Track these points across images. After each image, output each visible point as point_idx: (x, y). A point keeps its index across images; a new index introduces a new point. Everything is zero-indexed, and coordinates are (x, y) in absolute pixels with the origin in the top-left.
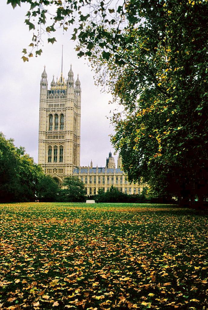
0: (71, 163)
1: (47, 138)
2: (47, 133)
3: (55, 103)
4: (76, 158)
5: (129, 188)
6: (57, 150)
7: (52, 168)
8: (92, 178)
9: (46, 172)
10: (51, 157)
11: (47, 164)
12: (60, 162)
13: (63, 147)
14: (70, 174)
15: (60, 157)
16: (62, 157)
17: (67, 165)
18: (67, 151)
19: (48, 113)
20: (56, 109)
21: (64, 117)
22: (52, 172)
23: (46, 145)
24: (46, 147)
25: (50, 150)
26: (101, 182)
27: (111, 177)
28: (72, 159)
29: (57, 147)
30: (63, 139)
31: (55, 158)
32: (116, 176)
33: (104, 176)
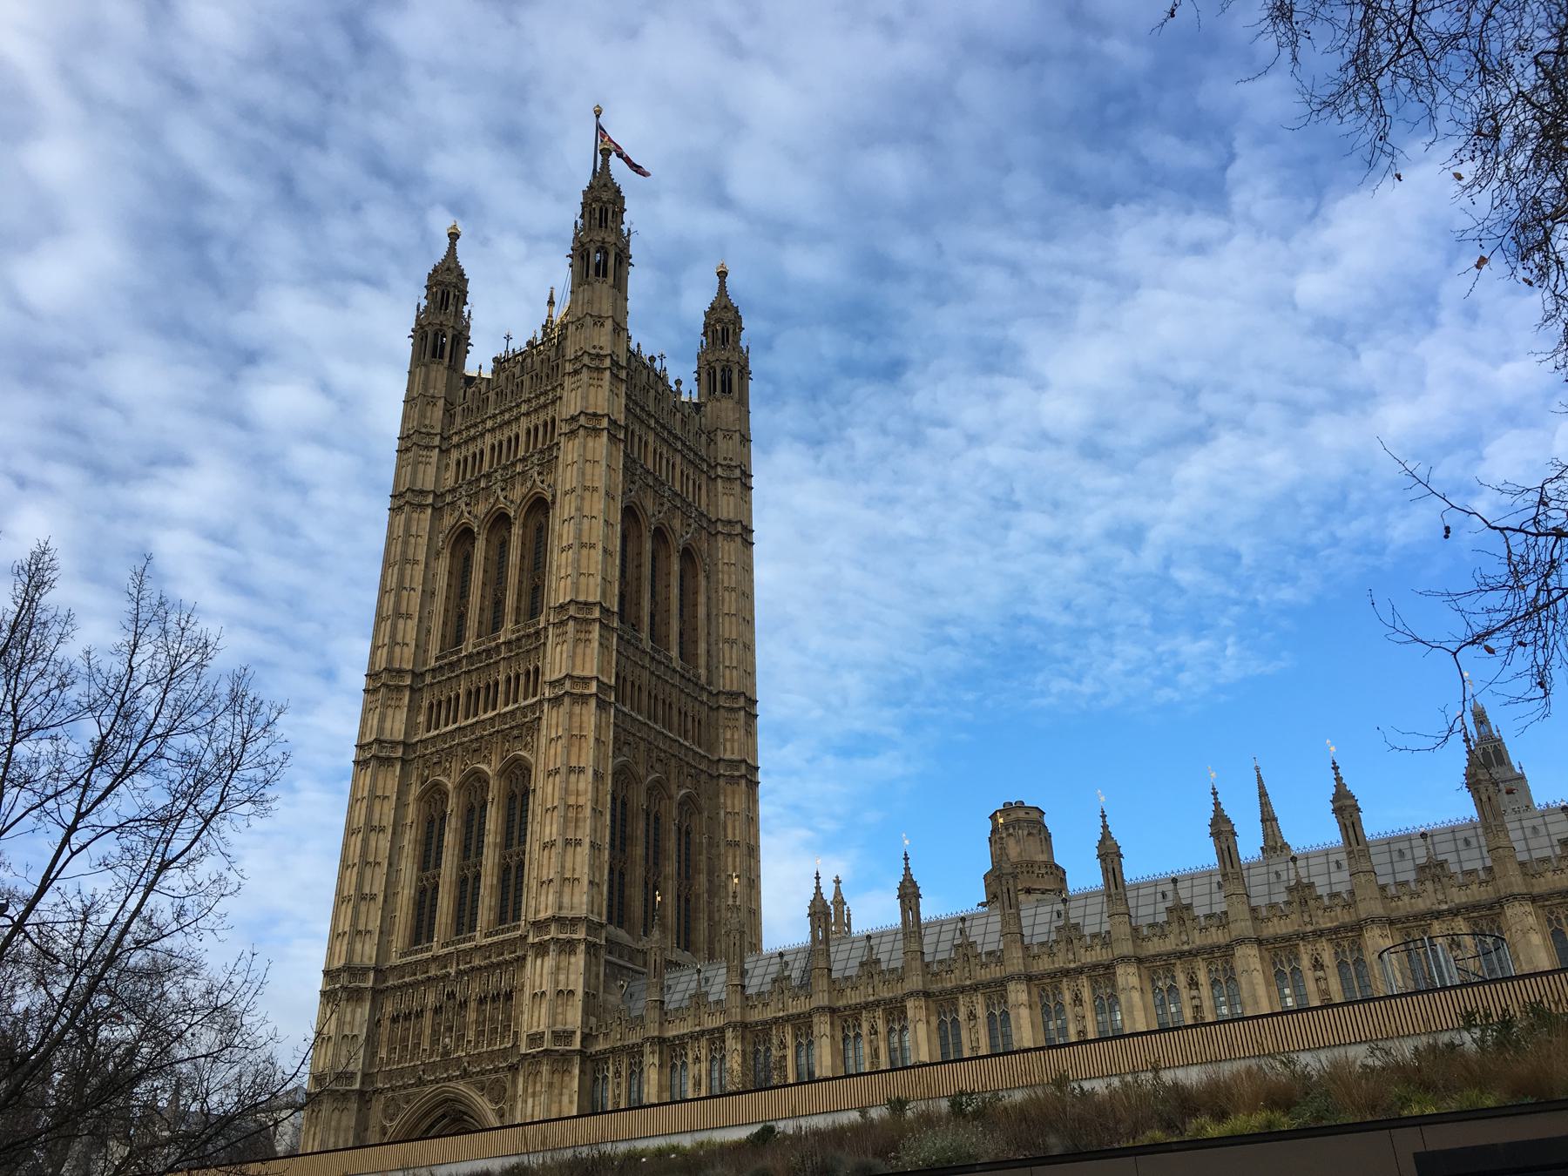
0: (579, 902)
1: (422, 719)
9: (383, 1053)
11: (395, 960)
14: (557, 1036)
16: (521, 865)
19: (448, 521)
24: (401, 805)
28: (583, 873)
31: (467, 886)
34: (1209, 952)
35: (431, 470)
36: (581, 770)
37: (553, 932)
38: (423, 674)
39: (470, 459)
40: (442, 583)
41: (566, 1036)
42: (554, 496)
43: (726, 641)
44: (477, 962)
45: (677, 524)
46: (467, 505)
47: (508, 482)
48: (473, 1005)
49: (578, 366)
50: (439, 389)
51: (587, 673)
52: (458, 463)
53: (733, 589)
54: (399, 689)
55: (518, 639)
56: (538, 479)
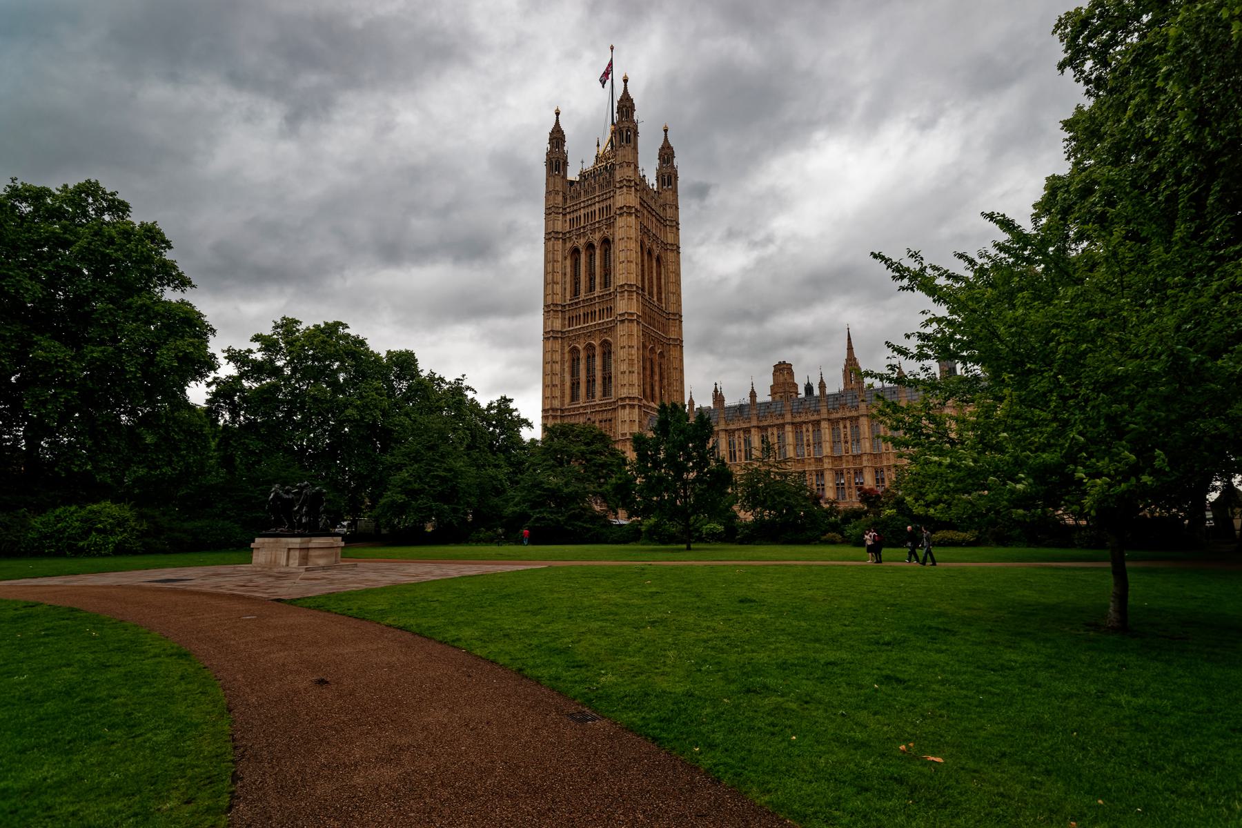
0: (635, 392)
1: (567, 323)
3: (587, 210)
5: (852, 472)
6: (594, 356)
10: (578, 383)
11: (566, 407)
12: (604, 395)
15: (604, 378)
16: (610, 378)
18: (622, 354)
19: (569, 245)
23: (563, 349)
24: (563, 354)
25: (575, 361)
28: (636, 382)
31: (591, 382)
32: (793, 424)
33: (750, 432)
34: (851, 419)
35: (560, 223)
36: (633, 347)
37: (627, 401)
38: (565, 306)
40: (568, 270)
43: (672, 293)
45: (654, 247)
47: (593, 231)
49: (622, 185)
50: (559, 188)
51: (632, 311)
54: (557, 311)
56: (606, 231)
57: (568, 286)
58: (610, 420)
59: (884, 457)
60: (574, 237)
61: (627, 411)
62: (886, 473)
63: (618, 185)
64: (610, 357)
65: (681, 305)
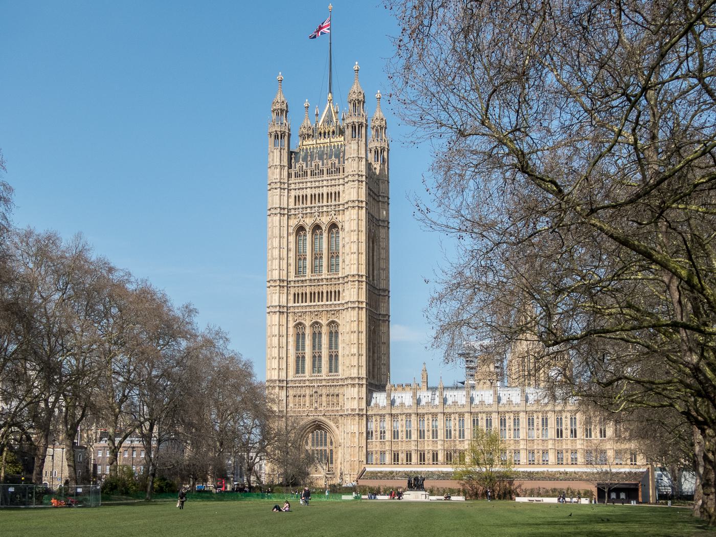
1: (291, 297)
2: (292, 284)
4: (379, 358)
5: (541, 452)
7: (308, 392)
8: (426, 422)
9: (291, 405)
10: (303, 357)
12: (330, 371)
13: (338, 325)
14: (359, 410)
15: (331, 356)
16: (337, 356)
17: (350, 381)
19: (294, 222)
20: (316, 208)
21: (340, 232)
22: (307, 404)
25: (300, 337)
26: (453, 432)
27: (485, 418)
29: (321, 325)
30: (337, 302)
31: (316, 358)
35: (286, 198)
39: (301, 198)
40: (292, 246)
41: (362, 410)
42: (342, 226)
44: (324, 383)
46: (302, 217)
48: (324, 396)
52: (295, 197)
53: (384, 249)
55: (331, 279)
56: (335, 217)
57: (292, 261)
58: (338, 395)
59: (564, 442)
60: (300, 215)
61: (356, 389)
62: (564, 454)
63: (350, 178)
64: (337, 337)
65: (389, 281)
